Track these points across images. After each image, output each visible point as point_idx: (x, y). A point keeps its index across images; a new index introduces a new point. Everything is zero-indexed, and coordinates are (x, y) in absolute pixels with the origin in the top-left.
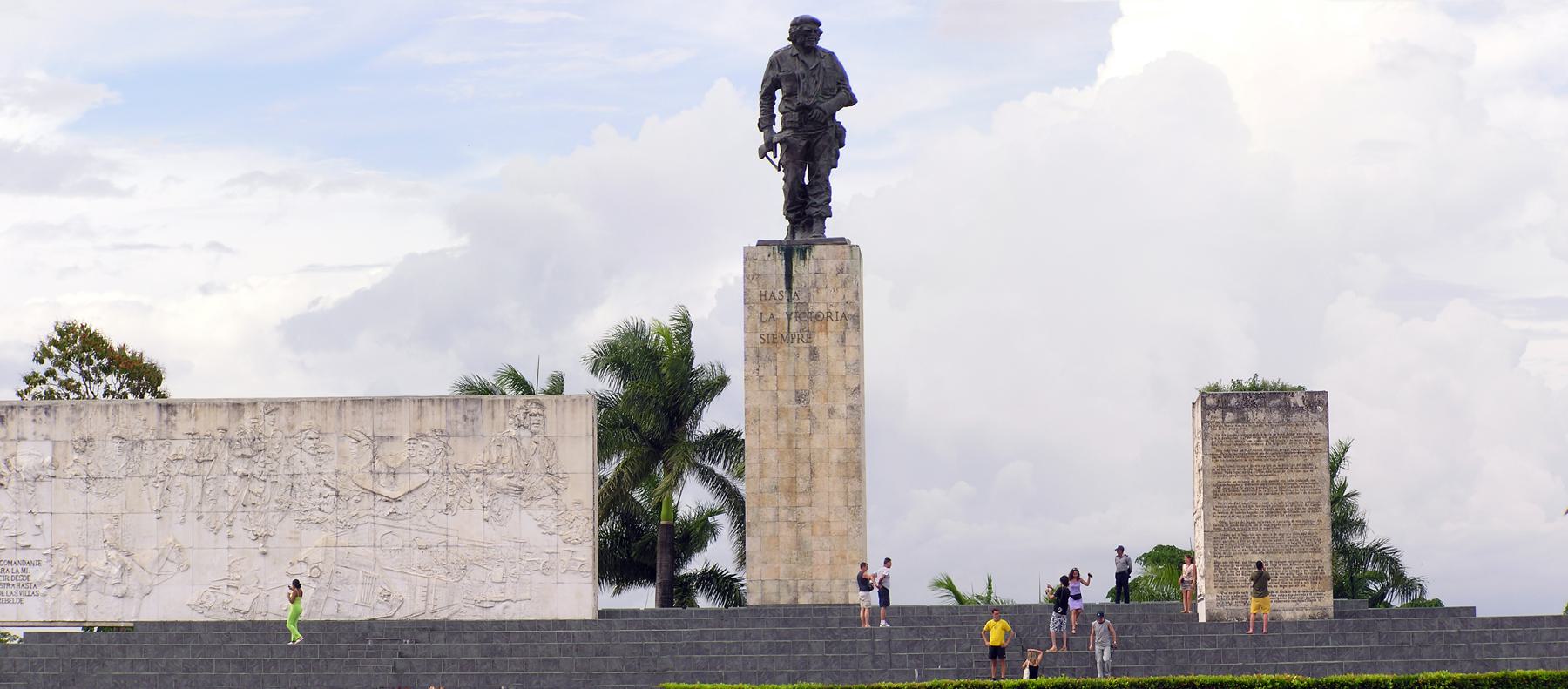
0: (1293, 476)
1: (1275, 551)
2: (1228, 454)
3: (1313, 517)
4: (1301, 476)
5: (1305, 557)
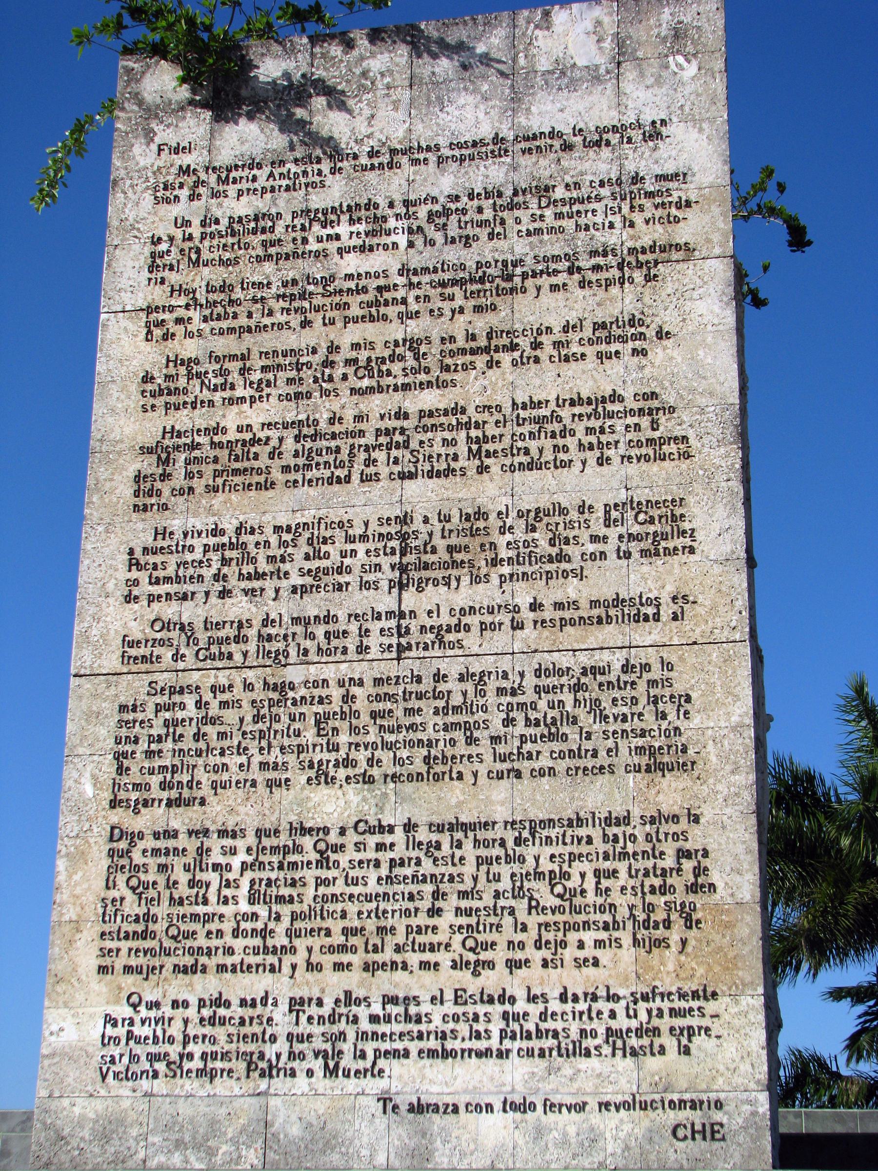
0: (546, 383)
1: (437, 769)
2: (220, 304)
3: (643, 578)
4: (588, 378)
5: (599, 796)
